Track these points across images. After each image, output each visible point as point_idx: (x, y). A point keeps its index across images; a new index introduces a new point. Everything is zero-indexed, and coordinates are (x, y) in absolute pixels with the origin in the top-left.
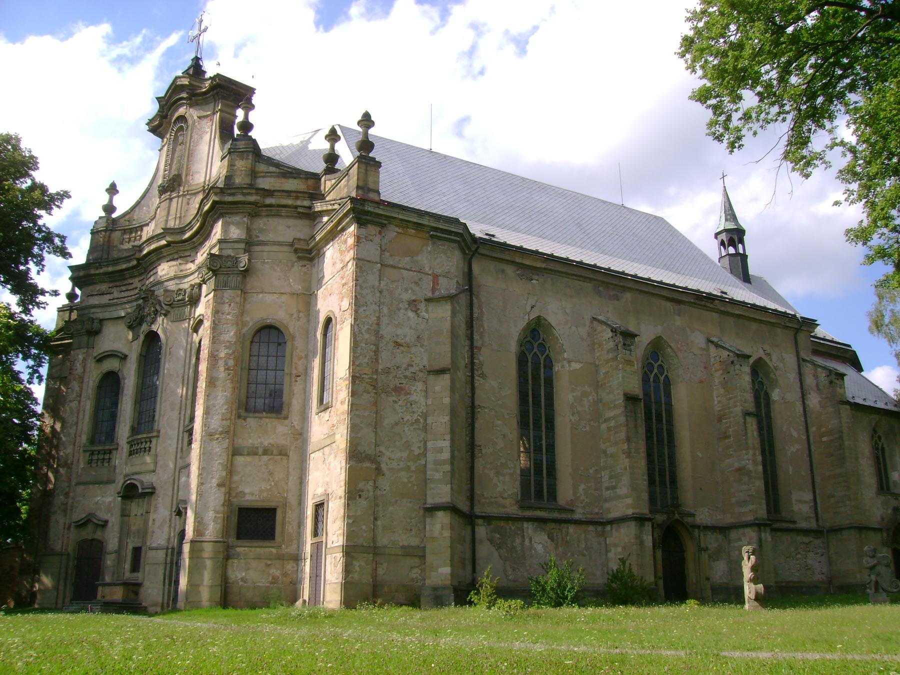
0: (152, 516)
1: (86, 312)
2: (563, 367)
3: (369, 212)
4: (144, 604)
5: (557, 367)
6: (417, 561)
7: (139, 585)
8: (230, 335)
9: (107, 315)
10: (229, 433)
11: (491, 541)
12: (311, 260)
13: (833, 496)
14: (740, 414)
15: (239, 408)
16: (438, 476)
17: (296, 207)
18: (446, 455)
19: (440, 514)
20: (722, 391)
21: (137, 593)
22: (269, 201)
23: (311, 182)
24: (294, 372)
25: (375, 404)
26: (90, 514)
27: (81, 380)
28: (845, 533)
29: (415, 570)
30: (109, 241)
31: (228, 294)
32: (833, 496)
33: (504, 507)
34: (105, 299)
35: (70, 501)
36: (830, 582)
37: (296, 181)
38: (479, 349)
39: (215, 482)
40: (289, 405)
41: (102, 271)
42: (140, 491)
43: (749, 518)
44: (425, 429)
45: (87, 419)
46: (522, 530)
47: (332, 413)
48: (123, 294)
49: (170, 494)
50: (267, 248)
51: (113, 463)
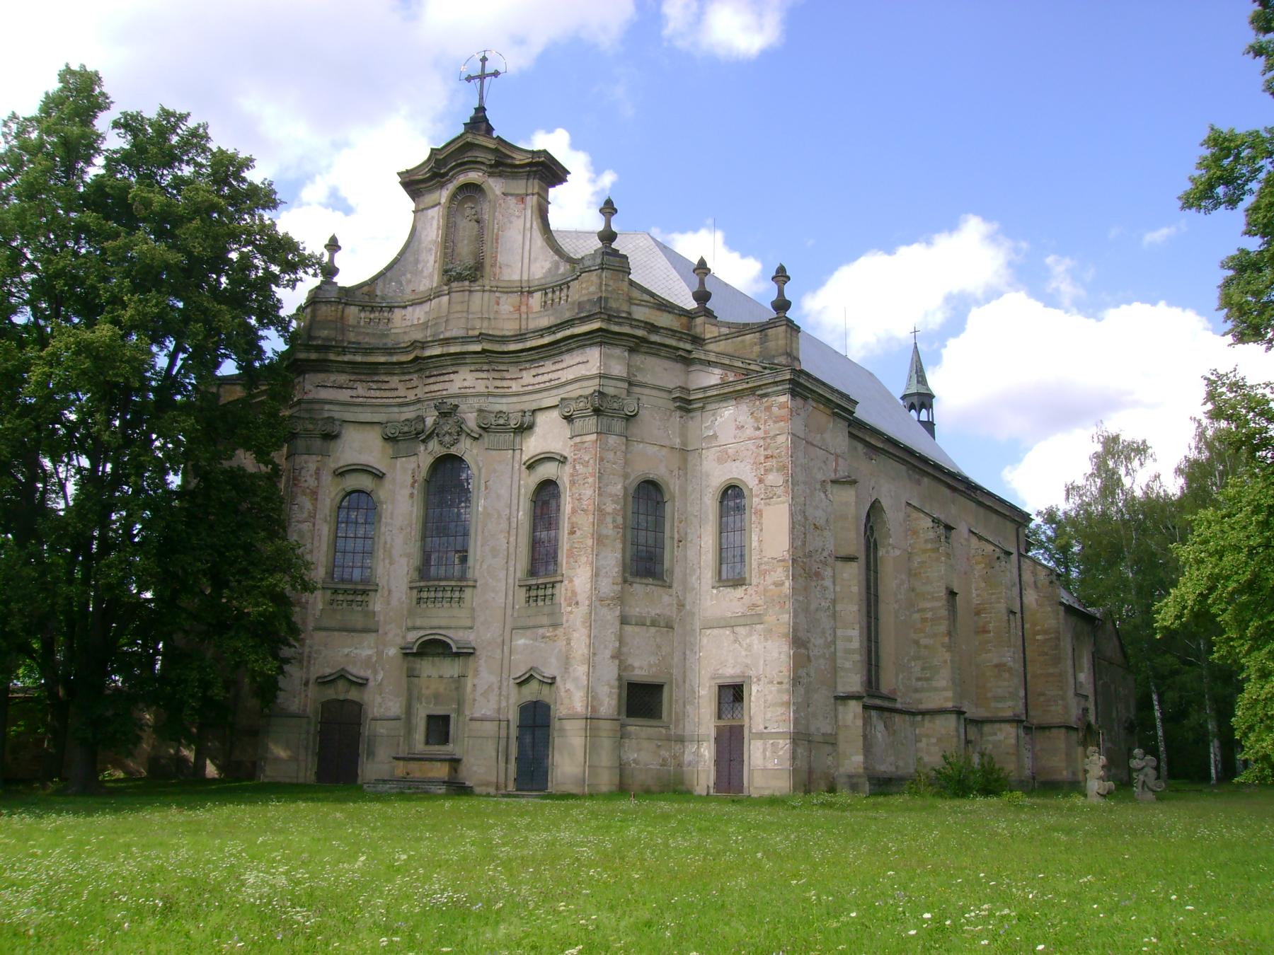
0: (469, 683)
1: (317, 407)
2: (887, 552)
3: (801, 384)
4: (468, 783)
5: (881, 553)
6: (828, 749)
7: (458, 761)
8: (617, 488)
9: (349, 416)
10: (621, 599)
12: (688, 411)
13: (1043, 694)
14: (1004, 611)
15: (624, 570)
16: (848, 665)
17: (678, 349)
18: (856, 644)
19: (853, 703)
20: (983, 585)
21: (456, 771)
22: (654, 338)
23: (684, 320)
24: (676, 536)
25: (805, 589)
26: (343, 669)
27: (314, 494)
28: (1053, 730)
29: (830, 758)
30: (342, 318)
31: (612, 440)
32: (1043, 694)
34: (344, 395)
35: (307, 650)
36: (1034, 778)
37: (670, 317)
39: (608, 653)
40: (672, 573)
41: (346, 358)
42: (454, 650)
43: (1008, 714)
44: (834, 616)
45: (324, 547)
47: (750, 591)
48: (373, 393)
49: (498, 656)
50: (647, 391)
51: (371, 607)
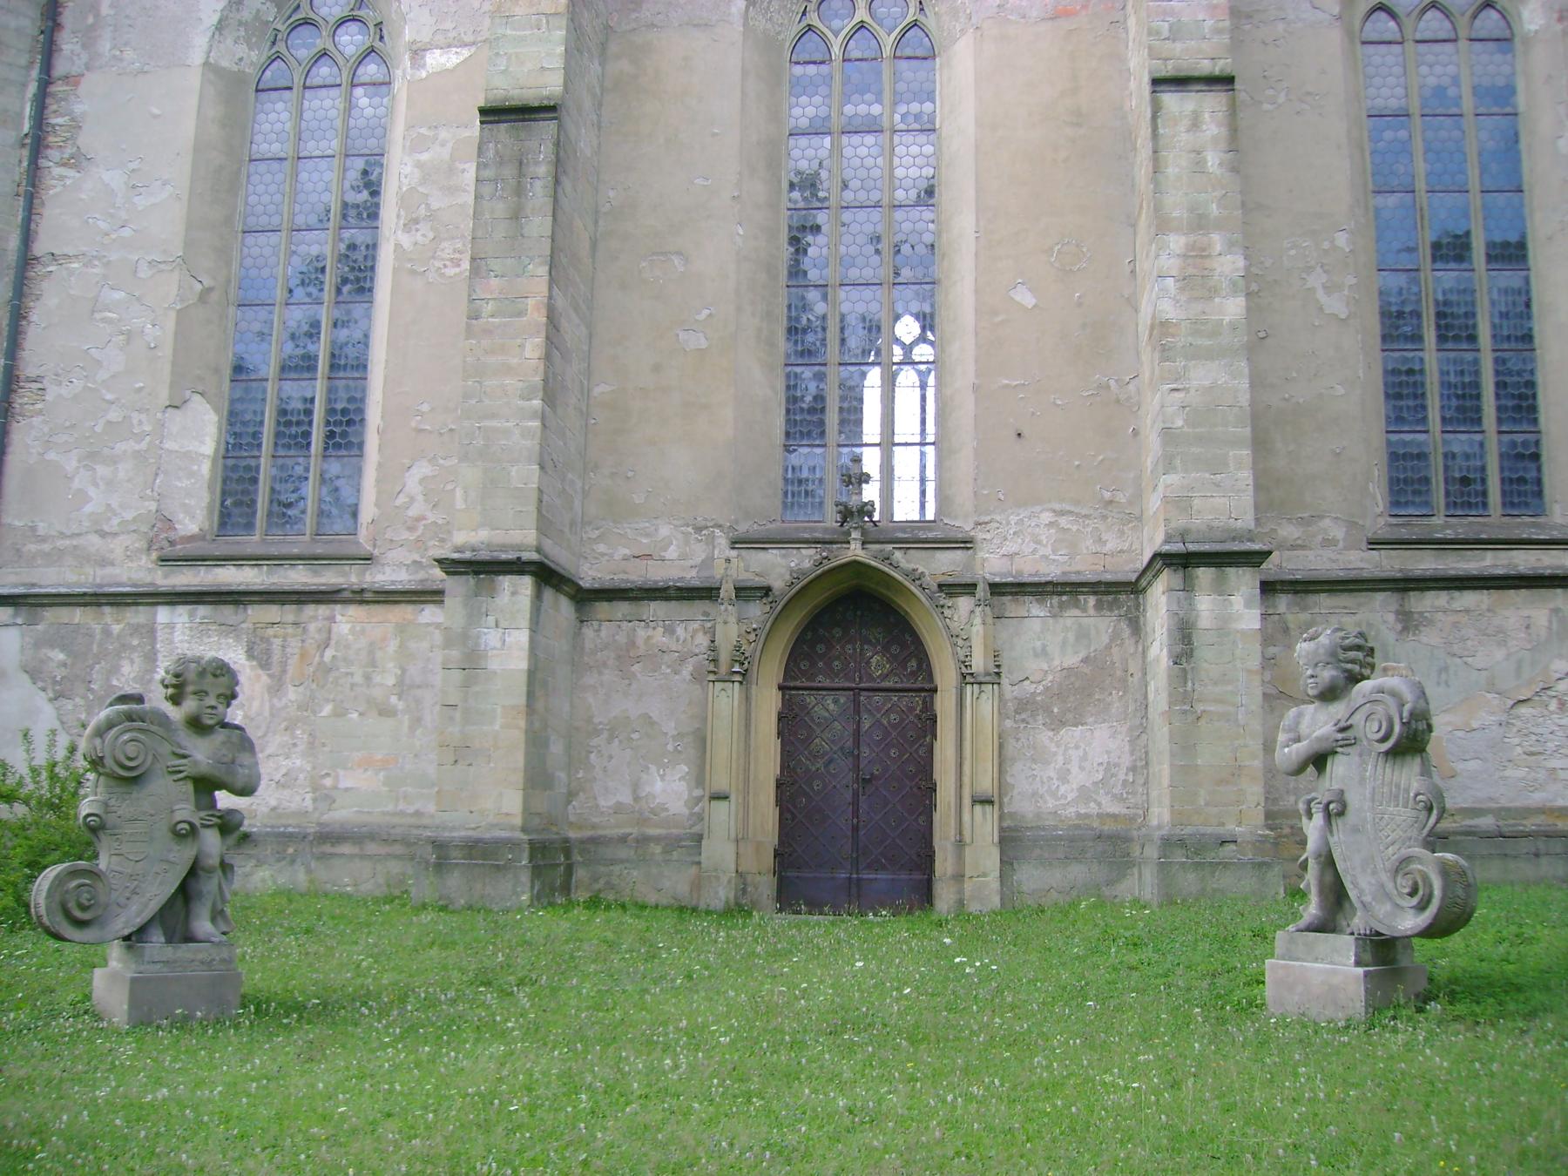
11: (34, 673)
33: (104, 562)
38: (72, 80)
46: (151, 631)
